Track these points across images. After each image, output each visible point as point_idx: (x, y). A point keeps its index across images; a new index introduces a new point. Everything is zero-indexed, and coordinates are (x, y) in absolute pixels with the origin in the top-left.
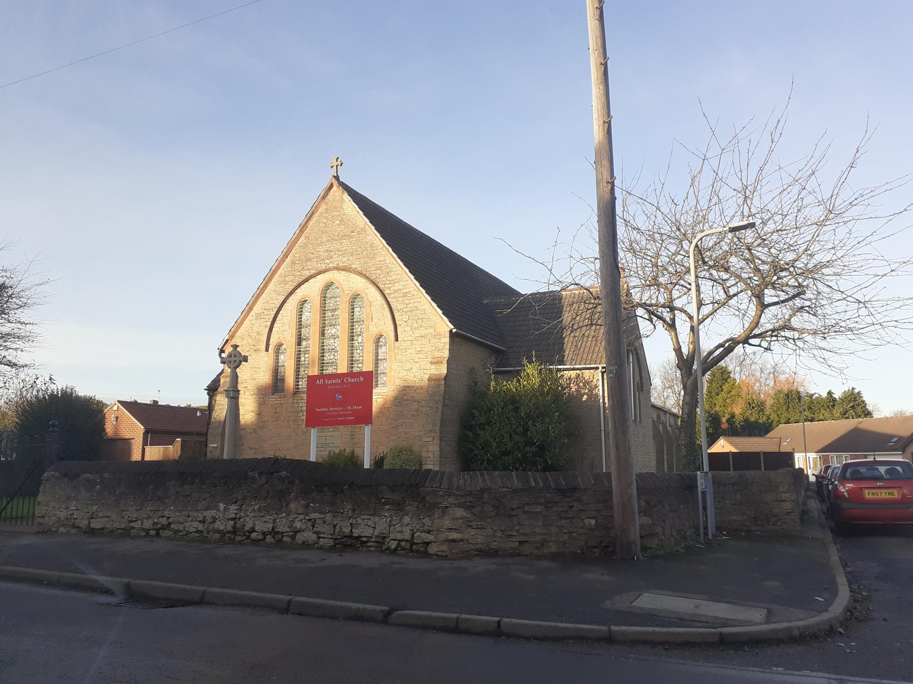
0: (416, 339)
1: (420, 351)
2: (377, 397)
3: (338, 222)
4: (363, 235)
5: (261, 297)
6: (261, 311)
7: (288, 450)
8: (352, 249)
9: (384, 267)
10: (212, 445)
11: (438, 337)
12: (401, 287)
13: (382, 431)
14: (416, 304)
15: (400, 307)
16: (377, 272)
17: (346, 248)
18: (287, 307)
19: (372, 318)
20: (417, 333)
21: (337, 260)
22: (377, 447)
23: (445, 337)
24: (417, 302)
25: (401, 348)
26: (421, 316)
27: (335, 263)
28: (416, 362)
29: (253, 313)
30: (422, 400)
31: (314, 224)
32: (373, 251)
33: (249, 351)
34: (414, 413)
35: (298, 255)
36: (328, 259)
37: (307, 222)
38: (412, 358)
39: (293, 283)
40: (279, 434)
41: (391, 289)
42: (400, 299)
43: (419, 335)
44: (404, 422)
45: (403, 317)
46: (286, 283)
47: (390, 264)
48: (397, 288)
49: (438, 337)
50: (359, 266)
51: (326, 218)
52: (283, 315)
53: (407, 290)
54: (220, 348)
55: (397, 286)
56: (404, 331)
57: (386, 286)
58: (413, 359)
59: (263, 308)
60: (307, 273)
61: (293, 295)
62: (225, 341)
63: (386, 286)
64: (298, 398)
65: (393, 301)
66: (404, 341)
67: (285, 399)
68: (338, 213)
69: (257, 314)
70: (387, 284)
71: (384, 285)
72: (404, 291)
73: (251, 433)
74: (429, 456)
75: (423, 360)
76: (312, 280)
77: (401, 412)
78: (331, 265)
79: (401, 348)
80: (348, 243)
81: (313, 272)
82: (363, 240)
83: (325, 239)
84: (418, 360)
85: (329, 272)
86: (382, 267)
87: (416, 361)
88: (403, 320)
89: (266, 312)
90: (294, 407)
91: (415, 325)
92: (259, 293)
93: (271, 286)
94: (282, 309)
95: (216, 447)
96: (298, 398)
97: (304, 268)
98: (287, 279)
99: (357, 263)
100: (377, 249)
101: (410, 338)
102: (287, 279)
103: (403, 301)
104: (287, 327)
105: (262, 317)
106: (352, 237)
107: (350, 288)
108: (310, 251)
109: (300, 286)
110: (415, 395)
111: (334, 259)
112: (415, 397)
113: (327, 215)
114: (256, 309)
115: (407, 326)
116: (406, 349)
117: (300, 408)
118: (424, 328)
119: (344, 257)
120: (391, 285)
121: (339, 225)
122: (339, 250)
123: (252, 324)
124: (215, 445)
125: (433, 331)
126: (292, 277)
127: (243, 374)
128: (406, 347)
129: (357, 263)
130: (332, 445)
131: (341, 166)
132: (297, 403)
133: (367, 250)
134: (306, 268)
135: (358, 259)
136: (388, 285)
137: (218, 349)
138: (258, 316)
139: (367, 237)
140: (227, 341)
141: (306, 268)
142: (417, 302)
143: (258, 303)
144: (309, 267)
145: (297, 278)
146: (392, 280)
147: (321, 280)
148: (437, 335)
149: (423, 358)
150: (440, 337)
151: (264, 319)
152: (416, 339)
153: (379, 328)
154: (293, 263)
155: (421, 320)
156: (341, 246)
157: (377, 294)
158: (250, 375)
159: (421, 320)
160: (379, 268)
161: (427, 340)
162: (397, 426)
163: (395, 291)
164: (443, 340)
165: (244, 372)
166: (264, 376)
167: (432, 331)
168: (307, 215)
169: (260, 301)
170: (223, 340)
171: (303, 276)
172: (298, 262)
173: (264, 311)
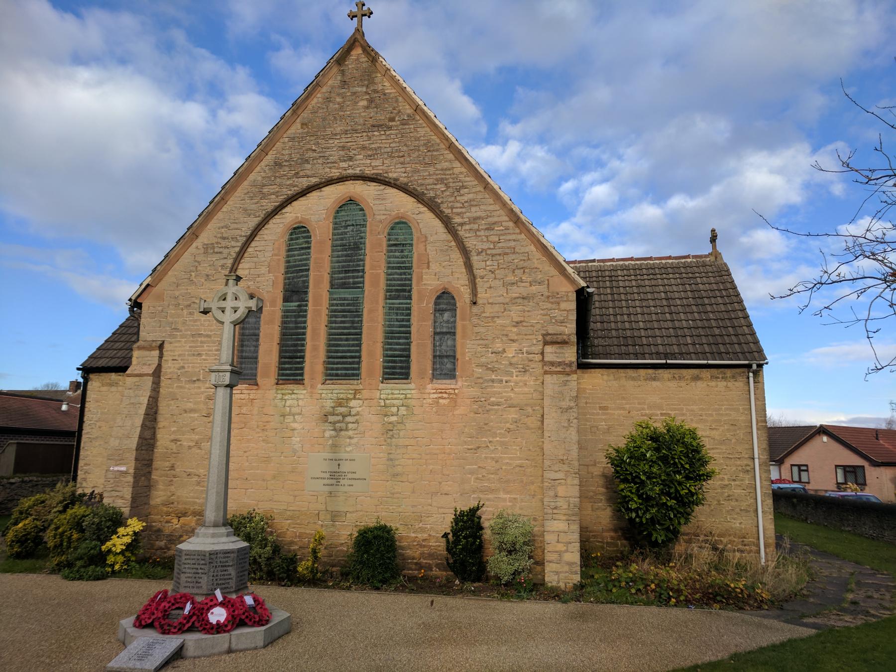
0: (513, 301)
1: (521, 322)
2: (440, 395)
3: (364, 103)
4: (412, 126)
5: (215, 218)
6: (215, 240)
7: (264, 480)
8: (390, 147)
9: (451, 180)
10: (116, 469)
11: (555, 300)
12: (483, 214)
13: (449, 454)
14: (512, 244)
15: (480, 246)
16: (438, 186)
17: (378, 145)
18: (265, 236)
19: (428, 263)
20: (515, 291)
21: (363, 165)
22: (440, 483)
23: (568, 301)
24: (514, 240)
25: (484, 315)
26: (522, 264)
27: (359, 169)
28: (513, 341)
29: (198, 243)
30: (527, 405)
31: (318, 103)
32: (430, 153)
33: (189, 306)
34: (511, 427)
35: (287, 152)
36: (345, 161)
37: (307, 98)
38: (505, 333)
39: (277, 197)
40: (245, 452)
41: (465, 216)
42: (482, 233)
43: (517, 295)
44: (490, 442)
45: (488, 263)
46: (264, 196)
47: (462, 176)
48: (475, 215)
49: (555, 300)
50: (404, 175)
51: (343, 96)
52: (256, 249)
53: (496, 219)
54: (133, 298)
55: (475, 212)
56: (490, 287)
57: (454, 210)
58: (507, 335)
59: (219, 235)
60: (304, 183)
61: (276, 217)
62: (143, 286)
63: (454, 210)
64: (283, 392)
65: (467, 235)
66: (489, 304)
67: (259, 391)
68: (364, 89)
69: (207, 245)
70: (457, 208)
71: (452, 208)
72: (490, 220)
73: (190, 447)
74: (559, 504)
75: (526, 337)
76: (315, 194)
77: (486, 424)
78: (350, 171)
79: (484, 315)
80: (383, 137)
81: (314, 180)
82: (411, 135)
83: (339, 129)
84: (516, 338)
85: (346, 182)
86: (446, 179)
87: (512, 338)
88: (487, 268)
89: (224, 243)
90: (276, 407)
91: (511, 278)
92: (213, 210)
93: (233, 202)
94: (256, 239)
95: (125, 473)
96: (283, 392)
97: (297, 173)
98: (265, 190)
99: (399, 170)
100: (437, 150)
101: (501, 300)
102: (265, 190)
103: (487, 237)
104: (264, 270)
105: (216, 250)
106: (390, 128)
107: (386, 210)
108: (309, 146)
109: (290, 203)
110: (512, 395)
111: (355, 162)
112: (511, 399)
113: (344, 90)
114: (206, 237)
115: (495, 279)
116: (493, 317)
117: (288, 409)
118: (528, 284)
119: (374, 159)
120: (463, 210)
121: (367, 107)
122: (364, 148)
123: (196, 261)
124: (123, 469)
125: (546, 290)
126: (275, 187)
127: (176, 345)
128: (492, 315)
129: (399, 170)
130: (350, 476)
131: (369, 17)
132: (282, 399)
133: (419, 150)
134: (301, 174)
135: (402, 163)
136: (459, 210)
137: (130, 300)
138: (208, 249)
139: (418, 129)
140: (148, 285)
141: (301, 174)
142: (514, 240)
143: (208, 227)
144: (309, 173)
145: (284, 190)
146: (466, 202)
147: (333, 194)
148: (554, 298)
149: (526, 335)
150: (558, 300)
151: (219, 255)
152: (514, 301)
153: (446, 280)
154: (278, 164)
155: (522, 270)
156: (368, 142)
157: (437, 224)
158: (190, 347)
159: (522, 270)
160: (441, 181)
161: (534, 304)
162: (479, 447)
163: (475, 219)
164: (563, 305)
165: (179, 341)
166: (217, 350)
167: (543, 288)
168: (307, 88)
169: (213, 225)
170: (140, 285)
171: (296, 186)
172: (287, 164)
173: (219, 240)
